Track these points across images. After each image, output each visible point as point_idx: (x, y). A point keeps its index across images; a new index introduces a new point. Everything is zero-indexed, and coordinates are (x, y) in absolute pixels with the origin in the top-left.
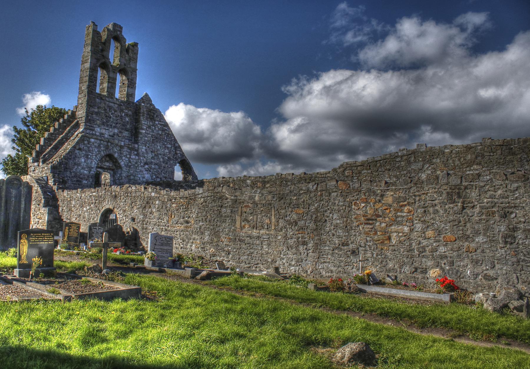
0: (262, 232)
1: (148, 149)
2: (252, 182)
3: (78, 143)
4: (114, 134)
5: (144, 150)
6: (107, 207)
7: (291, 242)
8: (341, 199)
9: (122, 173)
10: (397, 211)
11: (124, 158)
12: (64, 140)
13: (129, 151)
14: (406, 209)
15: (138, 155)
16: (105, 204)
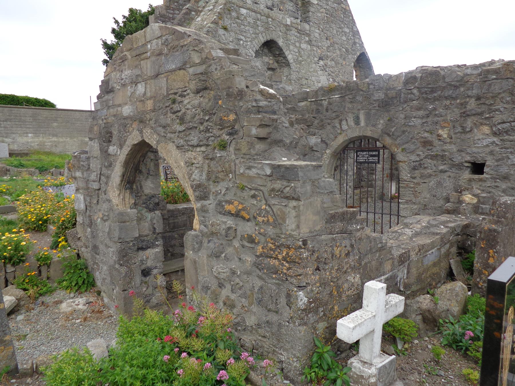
1: (322, 34)
3: (220, 16)
4: (273, 6)
5: (317, 35)
9: (290, 74)
11: (291, 47)
12: (193, 13)
13: (298, 35)
15: (309, 42)
16: (345, 127)
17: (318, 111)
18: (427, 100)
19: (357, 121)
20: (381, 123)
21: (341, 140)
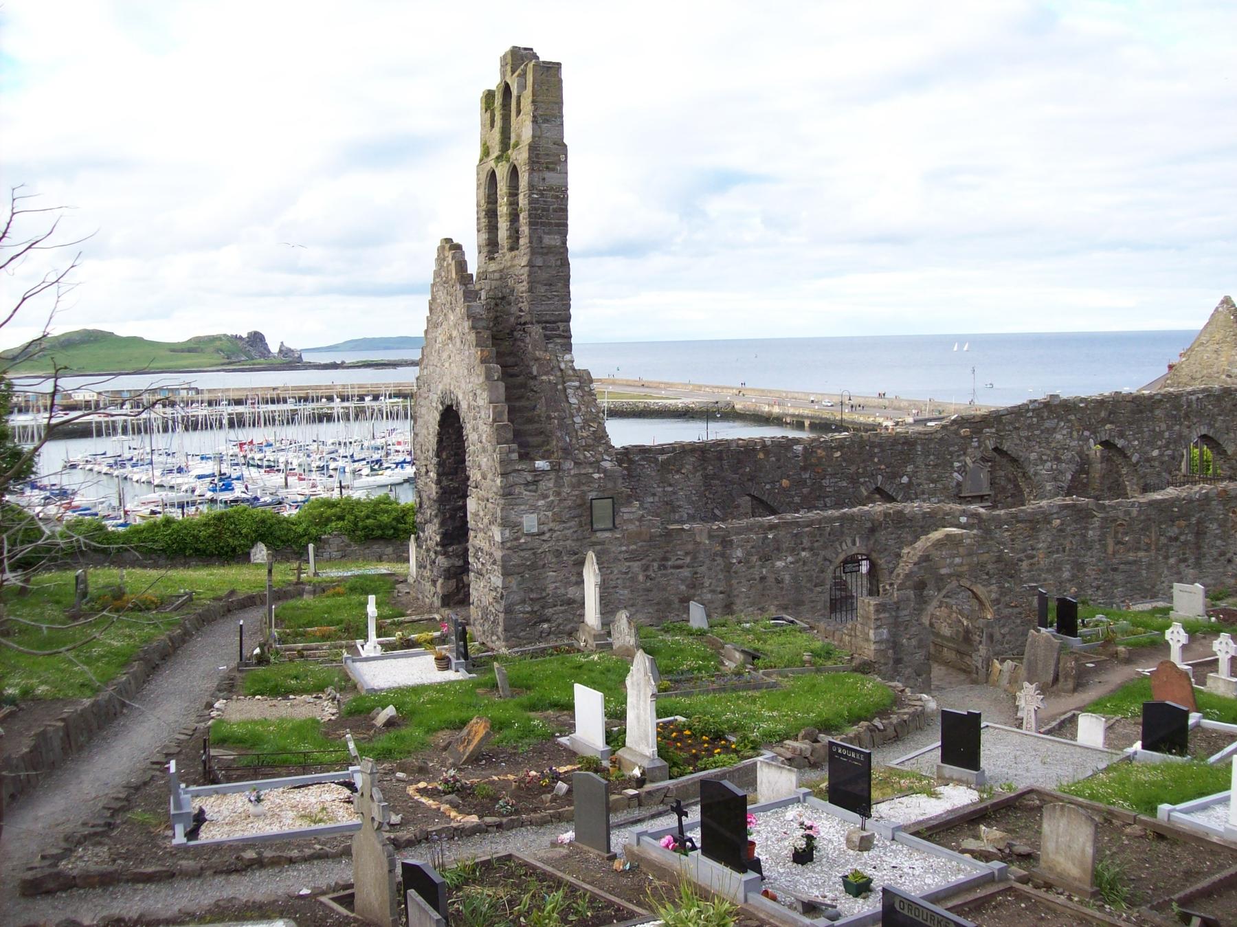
0: (1141, 554)
2: (805, 448)
6: (855, 550)
7: (1172, 561)
8: (1221, 507)
16: (844, 547)
19: (854, 543)
21: (842, 557)
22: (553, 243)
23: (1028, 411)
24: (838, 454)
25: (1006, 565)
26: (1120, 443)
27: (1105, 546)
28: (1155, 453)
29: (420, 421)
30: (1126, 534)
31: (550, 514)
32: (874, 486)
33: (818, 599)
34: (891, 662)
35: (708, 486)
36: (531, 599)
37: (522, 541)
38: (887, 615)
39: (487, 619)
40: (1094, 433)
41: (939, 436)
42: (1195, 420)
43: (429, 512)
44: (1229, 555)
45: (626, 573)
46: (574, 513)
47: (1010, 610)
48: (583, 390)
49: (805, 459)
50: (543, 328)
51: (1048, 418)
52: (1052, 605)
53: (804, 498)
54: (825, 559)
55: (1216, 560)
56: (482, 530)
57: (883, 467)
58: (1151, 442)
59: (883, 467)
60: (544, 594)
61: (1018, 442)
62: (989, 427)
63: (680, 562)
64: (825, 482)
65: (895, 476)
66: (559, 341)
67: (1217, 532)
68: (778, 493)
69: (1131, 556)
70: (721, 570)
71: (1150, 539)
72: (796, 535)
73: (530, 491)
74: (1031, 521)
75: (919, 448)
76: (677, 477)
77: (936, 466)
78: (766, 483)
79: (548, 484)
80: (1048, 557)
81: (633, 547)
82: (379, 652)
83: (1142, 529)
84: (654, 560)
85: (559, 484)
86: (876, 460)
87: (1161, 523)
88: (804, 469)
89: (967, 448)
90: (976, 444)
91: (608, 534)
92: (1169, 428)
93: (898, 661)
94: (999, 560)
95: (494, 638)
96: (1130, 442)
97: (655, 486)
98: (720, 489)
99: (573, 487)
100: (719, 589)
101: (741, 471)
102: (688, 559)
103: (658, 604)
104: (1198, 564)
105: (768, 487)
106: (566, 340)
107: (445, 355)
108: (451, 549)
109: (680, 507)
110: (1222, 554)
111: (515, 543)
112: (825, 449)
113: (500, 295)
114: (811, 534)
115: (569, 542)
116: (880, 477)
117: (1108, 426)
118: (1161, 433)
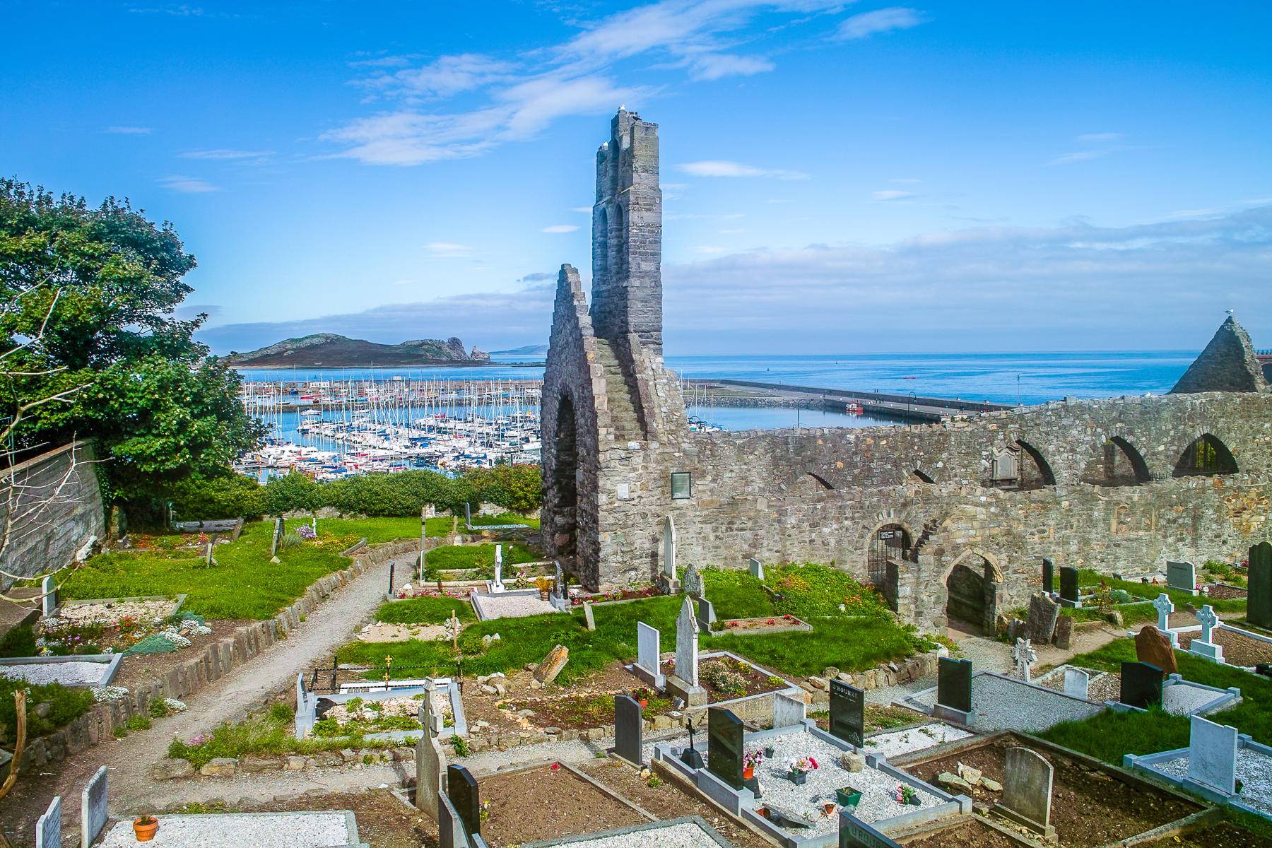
0: (1141, 533)
2: (857, 437)
7: (1170, 540)
8: (1217, 495)
10: (1258, 504)
14: (1264, 502)
16: (881, 518)
17: (861, 508)
18: (925, 504)
19: (889, 516)
20: (903, 516)
21: (879, 526)
22: (648, 269)
23: (1047, 410)
24: (885, 442)
25: (1014, 538)
26: (1129, 439)
27: (1109, 525)
28: (1162, 448)
29: (545, 408)
30: (1127, 515)
31: (638, 484)
32: (914, 469)
33: (858, 560)
34: (913, 615)
35: (776, 465)
36: (622, 552)
37: (616, 505)
38: (910, 575)
39: (588, 567)
40: (1106, 430)
41: (970, 429)
42: (1199, 421)
43: (550, 479)
44: (1224, 538)
45: (700, 533)
46: (659, 484)
47: (1018, 575)
48: (670, 386)
49: (857, 445)
50: (639, 336)
51: (1065, 417)
52: (1056, 574)
53: (855, 477)
54: (864, 527)
55: (1212, 541)
56: (586, 496)
57: (922, 454)
58: (1158, 440)
59: (922, 454)
60: (633, 548)
61: (1038, 436)
62: (1013, 423)
63: (743, 525)
64: (873, 465)
65: (931, 461)
66: (652, 346)
67: (1212, 516)
68: (834, 473)
69: (1133, 535)
70: (777, 533)
71: (1151, 521)
72: (840, 507)
73: (623, 465)
74: (1042, 502)
75: (953, 439)
76: (751, 457)
77: (967, 454)
78: (824, 465)
79: (638, 460)
80: (1058, 532)
81: (706, 512)
82: (501, 589)
83: (1143, 512)
84: (722, 523)
85: (646, 457)
86: (916, 448)
87: (1160, 507)
88: (855, 453)
89: (994, 440)
90: (1002, 437)
91: (686, 501)
92: (1175, 428)
93: (919, 614)
94: (1008, 533)
95: (593, 582)
96: (1138, 438)
97: (733, 464)
98: (785, 469)
99: (658, 462)
100: (775, 549)
101: (803, 454)
102: (750, 524)
103: (726, 559)
104: (1194, 543)
105: (825, 467)
106: (657, 346)
107: (563, 356)
108: (566, 510)
109: (752, 481)
110: (1218, 536)
111: (610, 506)
112: (873, 438)
113: (608, 309)
114: (852, 507)
115: (654, 507)
116: (919, 462)
117: (1118, 425)
118: (1167, 432)
